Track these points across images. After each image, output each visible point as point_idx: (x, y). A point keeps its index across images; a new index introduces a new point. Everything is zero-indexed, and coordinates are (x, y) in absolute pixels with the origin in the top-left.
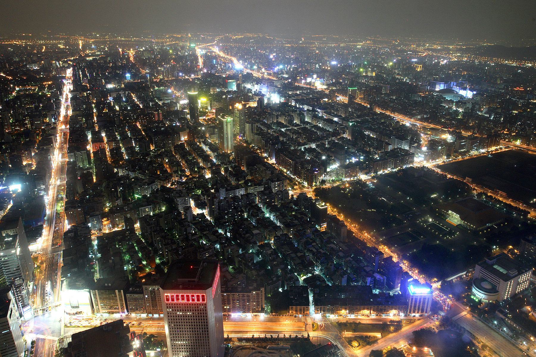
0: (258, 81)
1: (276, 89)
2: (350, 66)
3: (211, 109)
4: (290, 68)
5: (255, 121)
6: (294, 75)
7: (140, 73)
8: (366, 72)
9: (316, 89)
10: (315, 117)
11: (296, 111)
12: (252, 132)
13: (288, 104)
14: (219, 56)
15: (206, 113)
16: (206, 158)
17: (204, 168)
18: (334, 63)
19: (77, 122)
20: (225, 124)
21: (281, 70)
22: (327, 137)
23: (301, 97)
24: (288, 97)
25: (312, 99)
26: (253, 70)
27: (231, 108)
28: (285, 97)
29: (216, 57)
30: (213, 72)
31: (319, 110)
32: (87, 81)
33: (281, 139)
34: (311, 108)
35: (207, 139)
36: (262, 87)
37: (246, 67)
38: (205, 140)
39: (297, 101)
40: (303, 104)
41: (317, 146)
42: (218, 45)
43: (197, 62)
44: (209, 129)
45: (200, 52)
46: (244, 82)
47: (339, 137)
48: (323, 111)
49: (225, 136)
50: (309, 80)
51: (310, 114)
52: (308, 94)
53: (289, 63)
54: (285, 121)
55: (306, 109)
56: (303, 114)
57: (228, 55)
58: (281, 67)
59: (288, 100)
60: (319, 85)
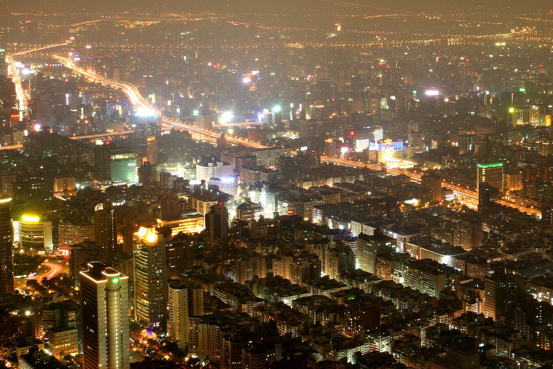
0: (209, 155)
1: (264, 177)
2: (478, 101)
3: (56, 247)
4: (303, 114)
5: (199, 277)
6: (317, 135)
8: (526, 118)
9: (384, 171)
10: (385, 256)
11: (327, 241)
12: (191, 315)
13: (301, 218)
14: (83, 81)
18: (432, 93)
21: (279, 117)
22: (425, 314)
23: (338, 197)
24: (299, 200)
25: (374, 202)
26: (191, 120)
27: (120, 240)
28: (290, 199)
29: (75, 84)
30: (63, 129)
31: (395, 236)
33: (283, 330)
34: (370, 231)
35: (41, 347)
36: (220, 171)
37: (169, 114)
38: (34, 350)
39: (327, 211)
40: (346, 219)
41: (395, 346)
42: (79, 50)
43: (11, 99)
44: (47, 313)
45: (18, 70)
46: (162, 158)
47: (457, 314)
48: (408, 237)
49: (103, 334)
50: (361, 145)
51: (369, 249)
52: (359, 188)
53: (299, 98)
54: (293, 274)
55: (355, 234)
56: (348, 250)
57: (110, 76)
58: (277, 109)
59: (301, 210)
60: (391, 157)
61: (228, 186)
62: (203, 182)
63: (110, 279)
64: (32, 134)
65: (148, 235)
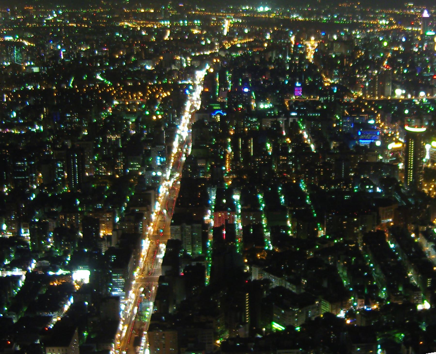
7: (322, 85)
17: (414, 288)
19: (196, 169)
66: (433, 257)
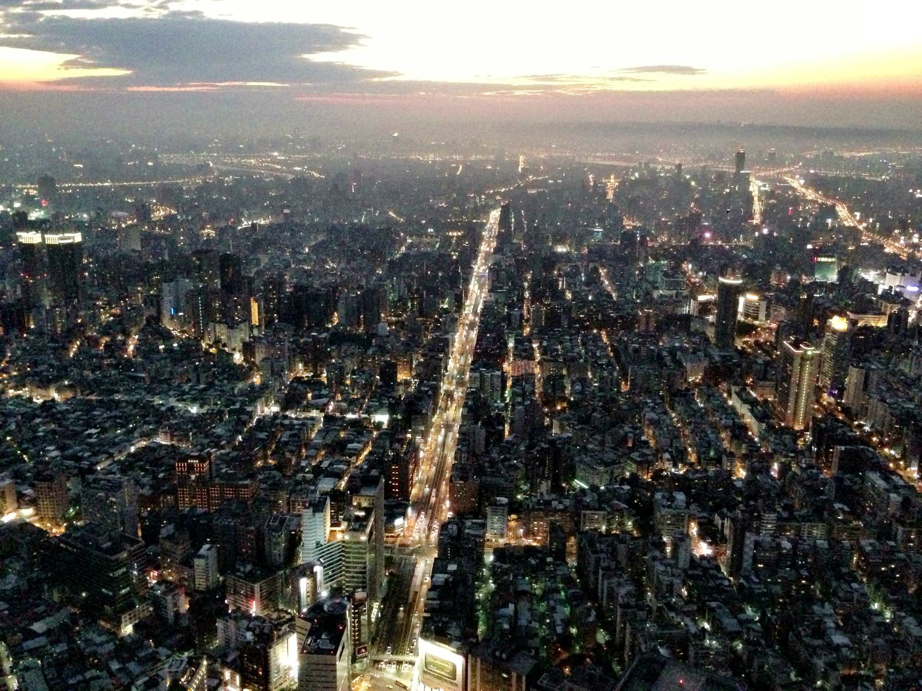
15: (754, 327)
16: (739, 432)
17: (731, 455)
20: (797, 362)
32: (521, 235)
35: (748, 389)
61: (913, 293)
62: (891, 287)
63: (806, 351)
64: (762, 235)
65: (839, 324)
66: (748, 420)
